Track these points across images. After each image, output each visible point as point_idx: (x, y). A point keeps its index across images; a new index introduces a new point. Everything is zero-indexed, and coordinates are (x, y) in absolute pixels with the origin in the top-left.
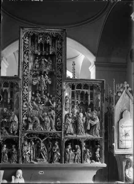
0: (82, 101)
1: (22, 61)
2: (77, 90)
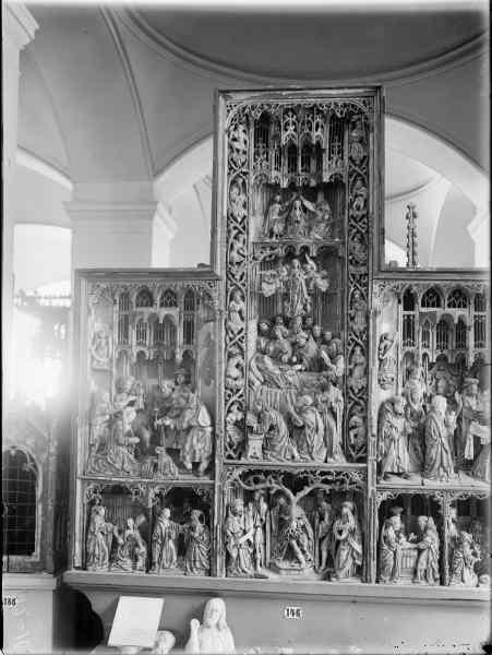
2: (424, 310)
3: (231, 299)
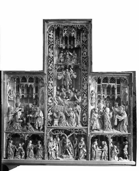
0: (109, 95)
1: (47, 56)
2: (103, 84)
3: (49, 80)
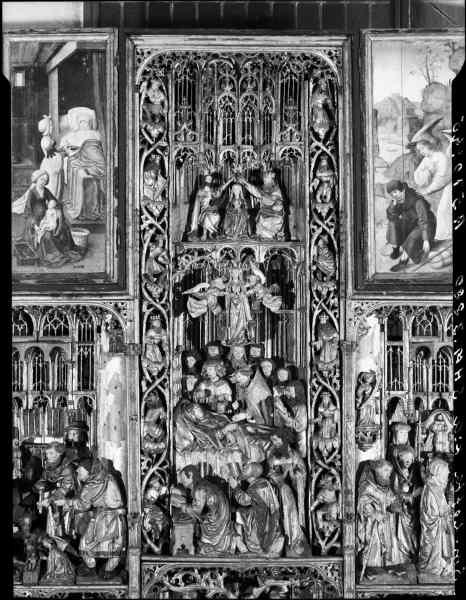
3: (148, 329)
